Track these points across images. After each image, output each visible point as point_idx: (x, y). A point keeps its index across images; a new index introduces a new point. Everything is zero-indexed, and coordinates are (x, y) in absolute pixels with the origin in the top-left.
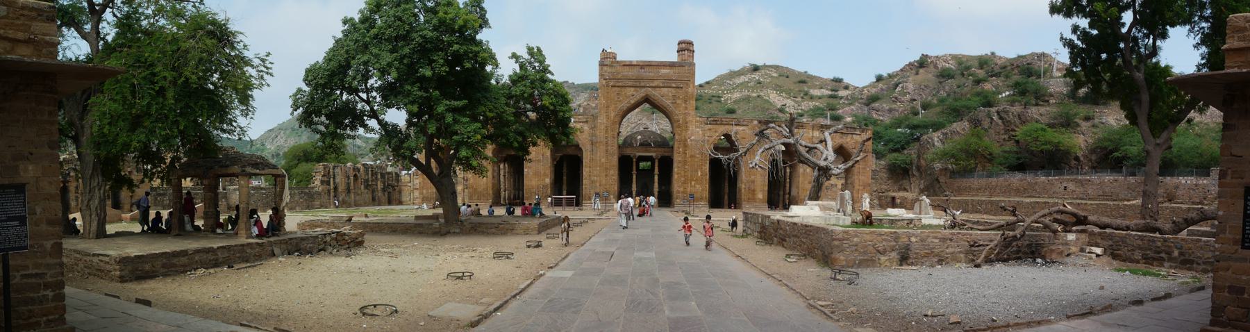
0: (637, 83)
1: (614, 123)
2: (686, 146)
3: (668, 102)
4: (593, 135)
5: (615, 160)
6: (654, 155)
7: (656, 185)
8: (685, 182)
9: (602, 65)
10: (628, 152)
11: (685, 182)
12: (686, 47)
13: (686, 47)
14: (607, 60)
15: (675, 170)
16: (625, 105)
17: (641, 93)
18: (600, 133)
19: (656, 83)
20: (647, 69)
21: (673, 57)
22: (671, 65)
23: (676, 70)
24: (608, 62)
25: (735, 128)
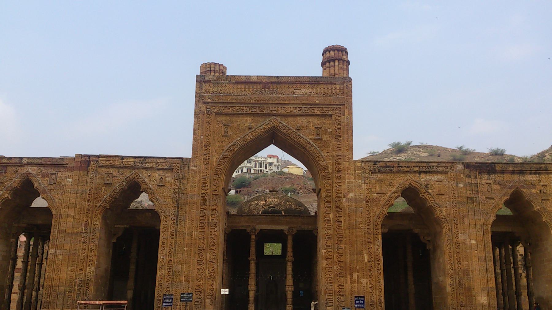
0: (258, 109)
1: (217, 172)
2: (339, 209)
3: (309, 138)
4: (179, 191)
5: (219, 236)
6: (285, 228)
7: (290, 281)
8: (339, 275)
9: (201, 80)
10: (243, 224)
11: (339, 275)
12: (335, 57)
13: (335, 57)
14: (211, 79)
15: (322, 252)
16: (237, 140)
17: (262, 125)
18: (193, 189)
19: (288, 109)
20: (273, 88)
21: (317, 71)
22: (313, 81)
23: (321, 89)
24: (211, 76)
25: (423, 178)
